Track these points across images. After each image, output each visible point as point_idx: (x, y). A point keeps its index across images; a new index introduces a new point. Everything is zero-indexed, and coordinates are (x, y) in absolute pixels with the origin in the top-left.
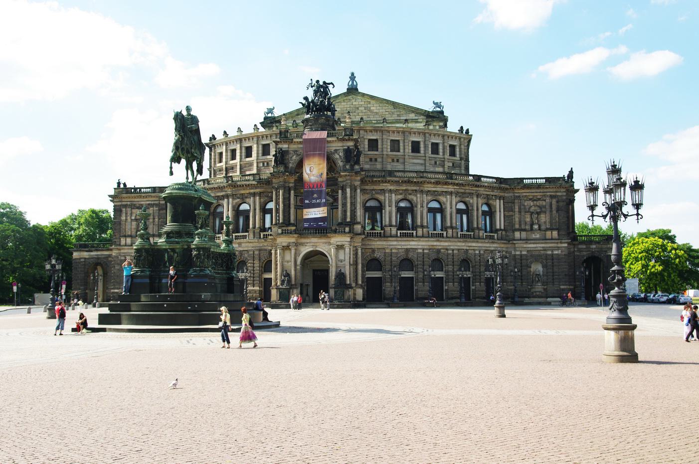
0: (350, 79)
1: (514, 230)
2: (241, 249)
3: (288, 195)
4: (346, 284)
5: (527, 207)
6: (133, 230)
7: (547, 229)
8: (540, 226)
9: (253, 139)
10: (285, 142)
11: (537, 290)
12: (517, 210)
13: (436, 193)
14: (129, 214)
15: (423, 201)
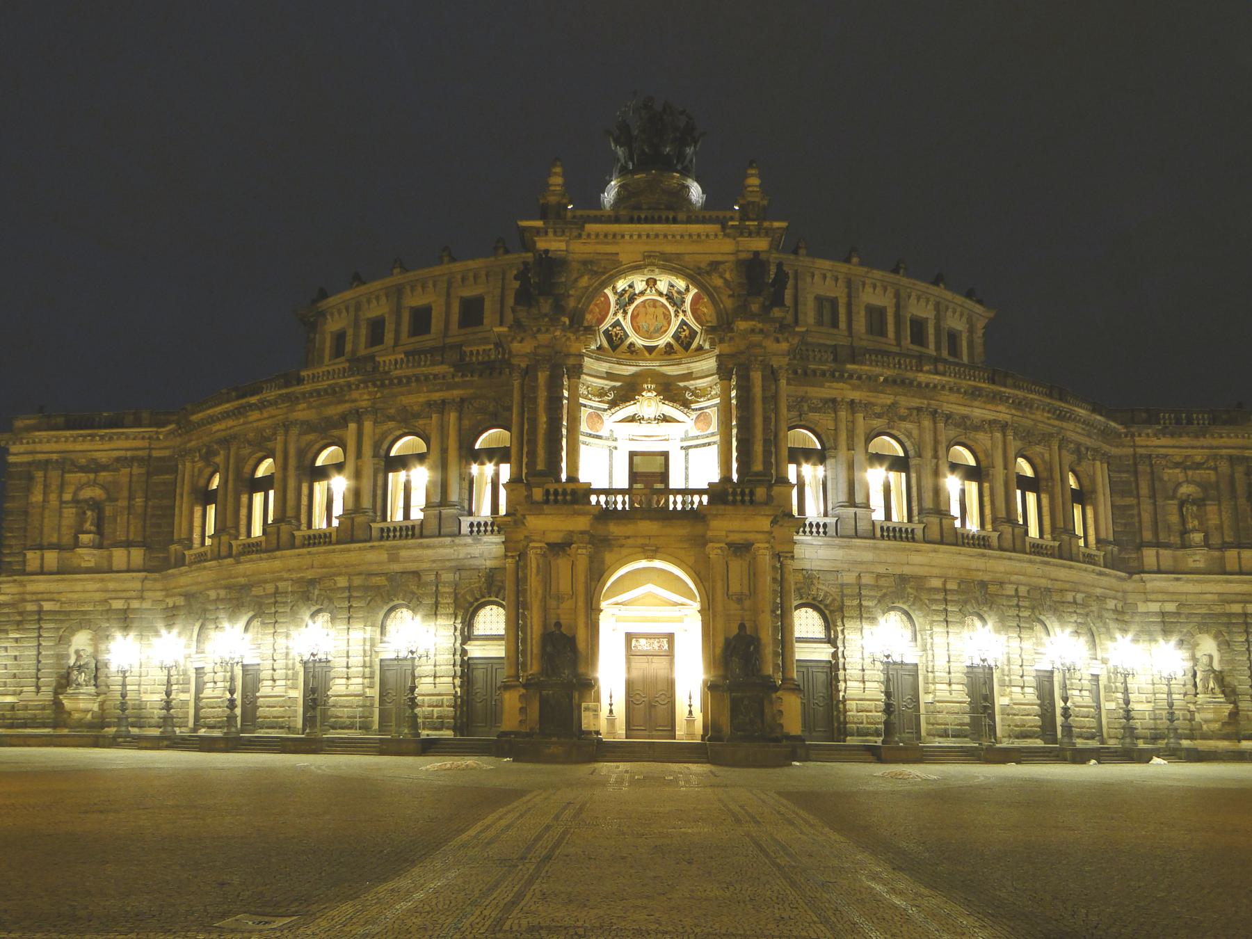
2: (396, 567)
9: (434, 286)
12: (1144, 490)
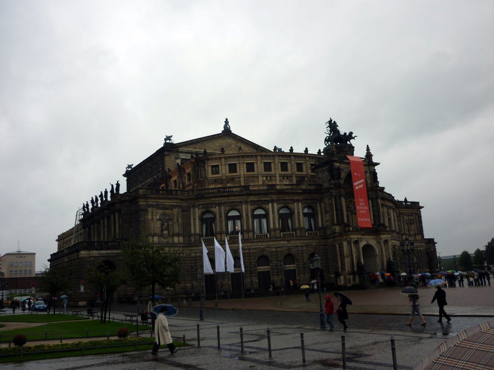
0: (225, 123)
1: (402, 235)
7: (415, 235)
12: (402, 221)
14: (154, 214)
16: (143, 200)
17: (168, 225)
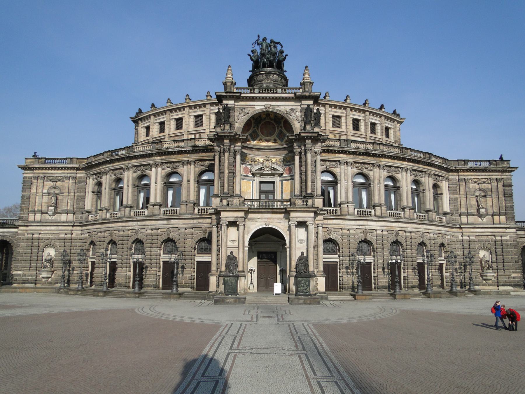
2: (171, 226)
3: (233, 159)
4: (309, 272)
5: (472, 190)
6: (43, 204)
8: (486, 209)
10: (231, 98)
11: (488, 277)
13: (392, 168)
15: (380, 177)
16: (29, 171)
17: (57, 199)
